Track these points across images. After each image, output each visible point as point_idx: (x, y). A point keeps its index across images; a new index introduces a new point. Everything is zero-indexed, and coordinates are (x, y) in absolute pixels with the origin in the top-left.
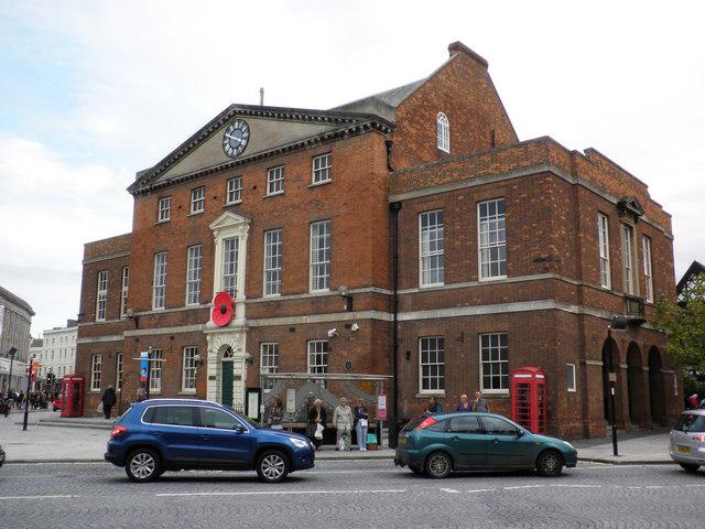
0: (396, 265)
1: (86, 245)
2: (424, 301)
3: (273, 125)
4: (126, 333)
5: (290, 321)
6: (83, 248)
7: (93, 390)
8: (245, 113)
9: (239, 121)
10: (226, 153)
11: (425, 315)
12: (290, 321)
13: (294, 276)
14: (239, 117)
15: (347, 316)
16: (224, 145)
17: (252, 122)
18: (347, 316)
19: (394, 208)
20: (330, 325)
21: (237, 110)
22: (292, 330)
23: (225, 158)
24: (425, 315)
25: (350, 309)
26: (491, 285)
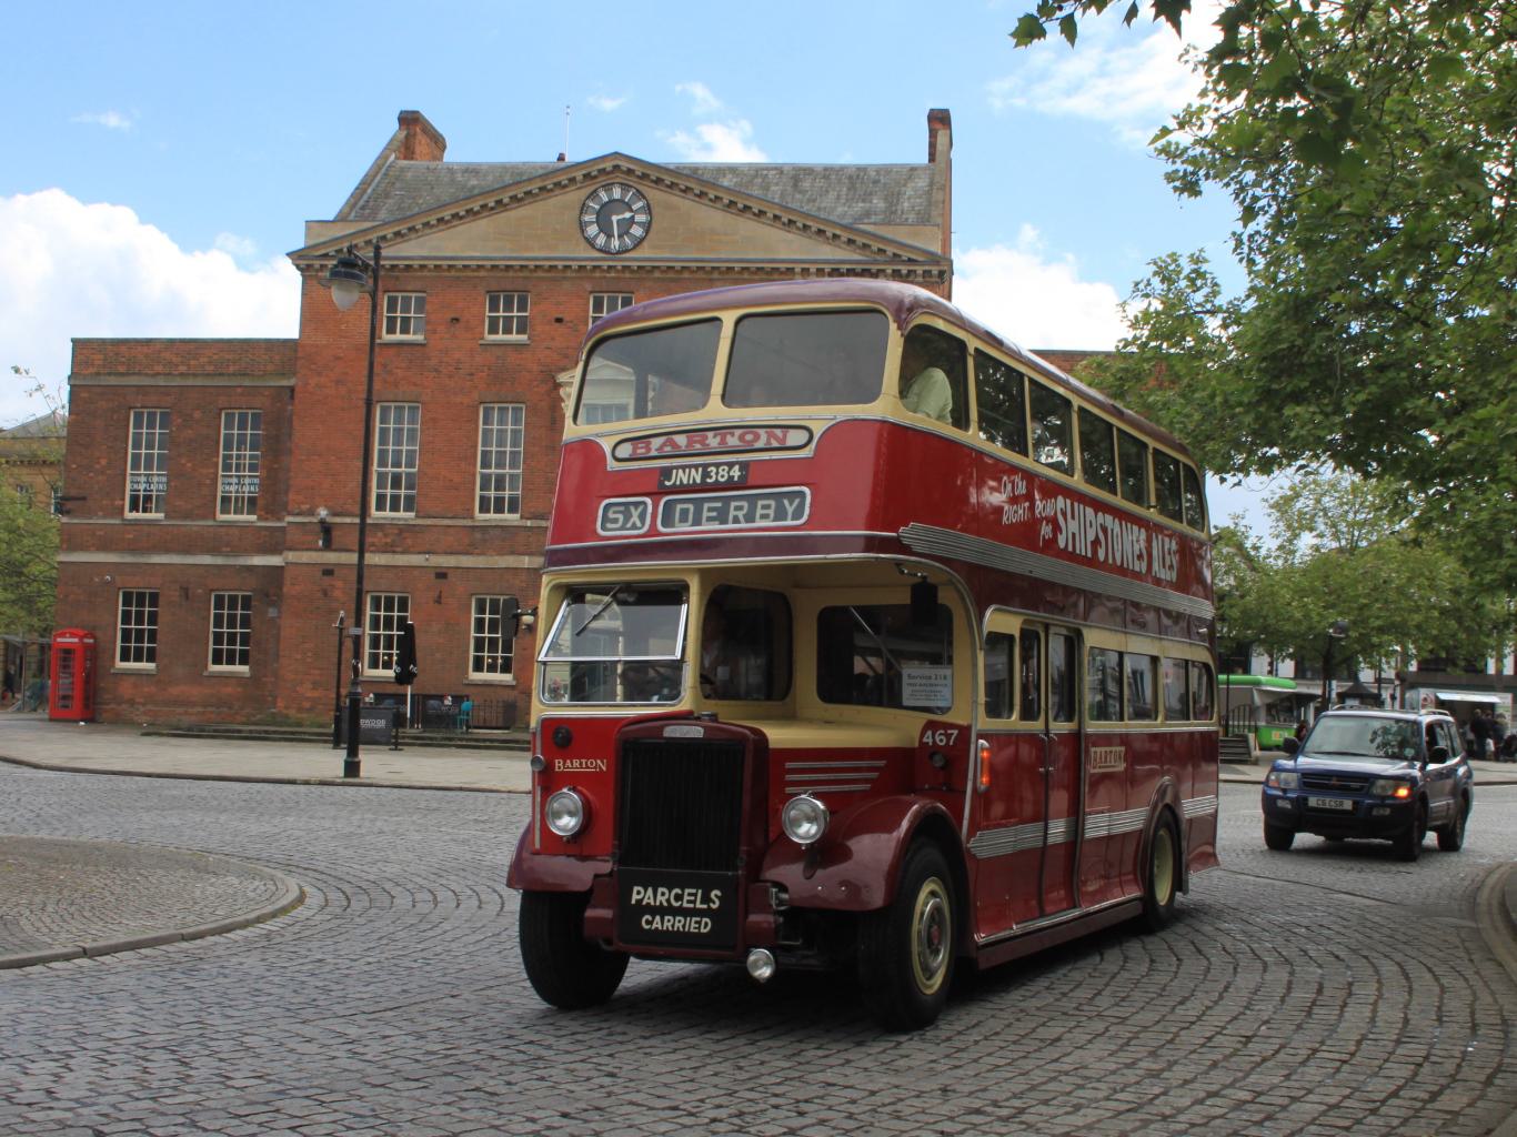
1: (79, 345)
4: (291, 556)
6: (68, 348)
7: (121, 665)
8: (644, 176)
9: (625, 187)
10: (591, 242)
14: (631, 181)
16: (582, 226)
17: (655, 195)
21: (625, 165)
23: (585, 252)
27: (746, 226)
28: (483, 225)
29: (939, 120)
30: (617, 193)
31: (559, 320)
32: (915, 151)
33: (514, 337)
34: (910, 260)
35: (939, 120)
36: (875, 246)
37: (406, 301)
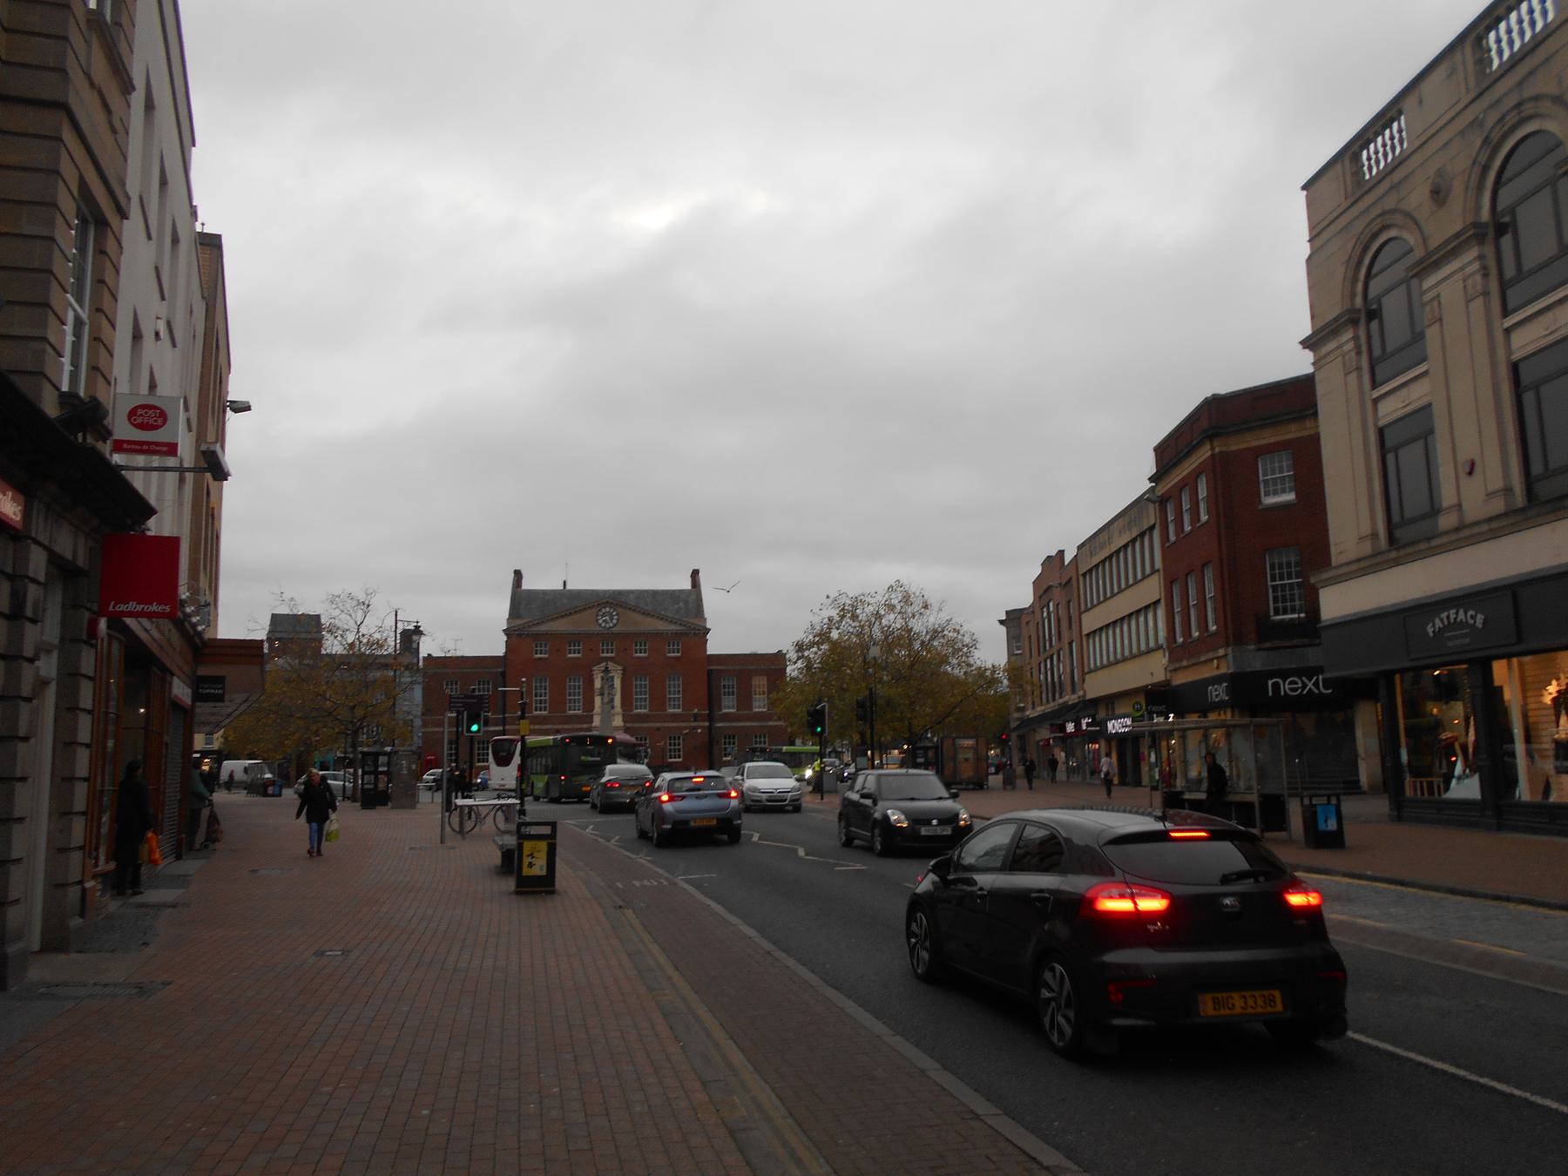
0: (712, 703)
2: (727, 717)
3: (638, 617)
5: (658, 725)
9: (611, 608)
10: (600, 625)
11: (727, 724)
12: (658, 725)
13: (658, 700)
15: (693, 724)
16: (597, 620)
17: (620, 610)
18: (693, 724)
19: (710, 673)
20: (686, 728)
22: (658, 729)
23: (598, 628)
24: (727, 724)
25: (695, 721)
26: (759, 712)
27: (649, 619)
28: (564, 620)
29: (695, 574)
30: (608, 609)
31: (591, 650)
32: (686, 585)
33: (576, 655)
34: (699, 630)
35: (695, 574)
36: (688, 625)
37: (541, 644)
